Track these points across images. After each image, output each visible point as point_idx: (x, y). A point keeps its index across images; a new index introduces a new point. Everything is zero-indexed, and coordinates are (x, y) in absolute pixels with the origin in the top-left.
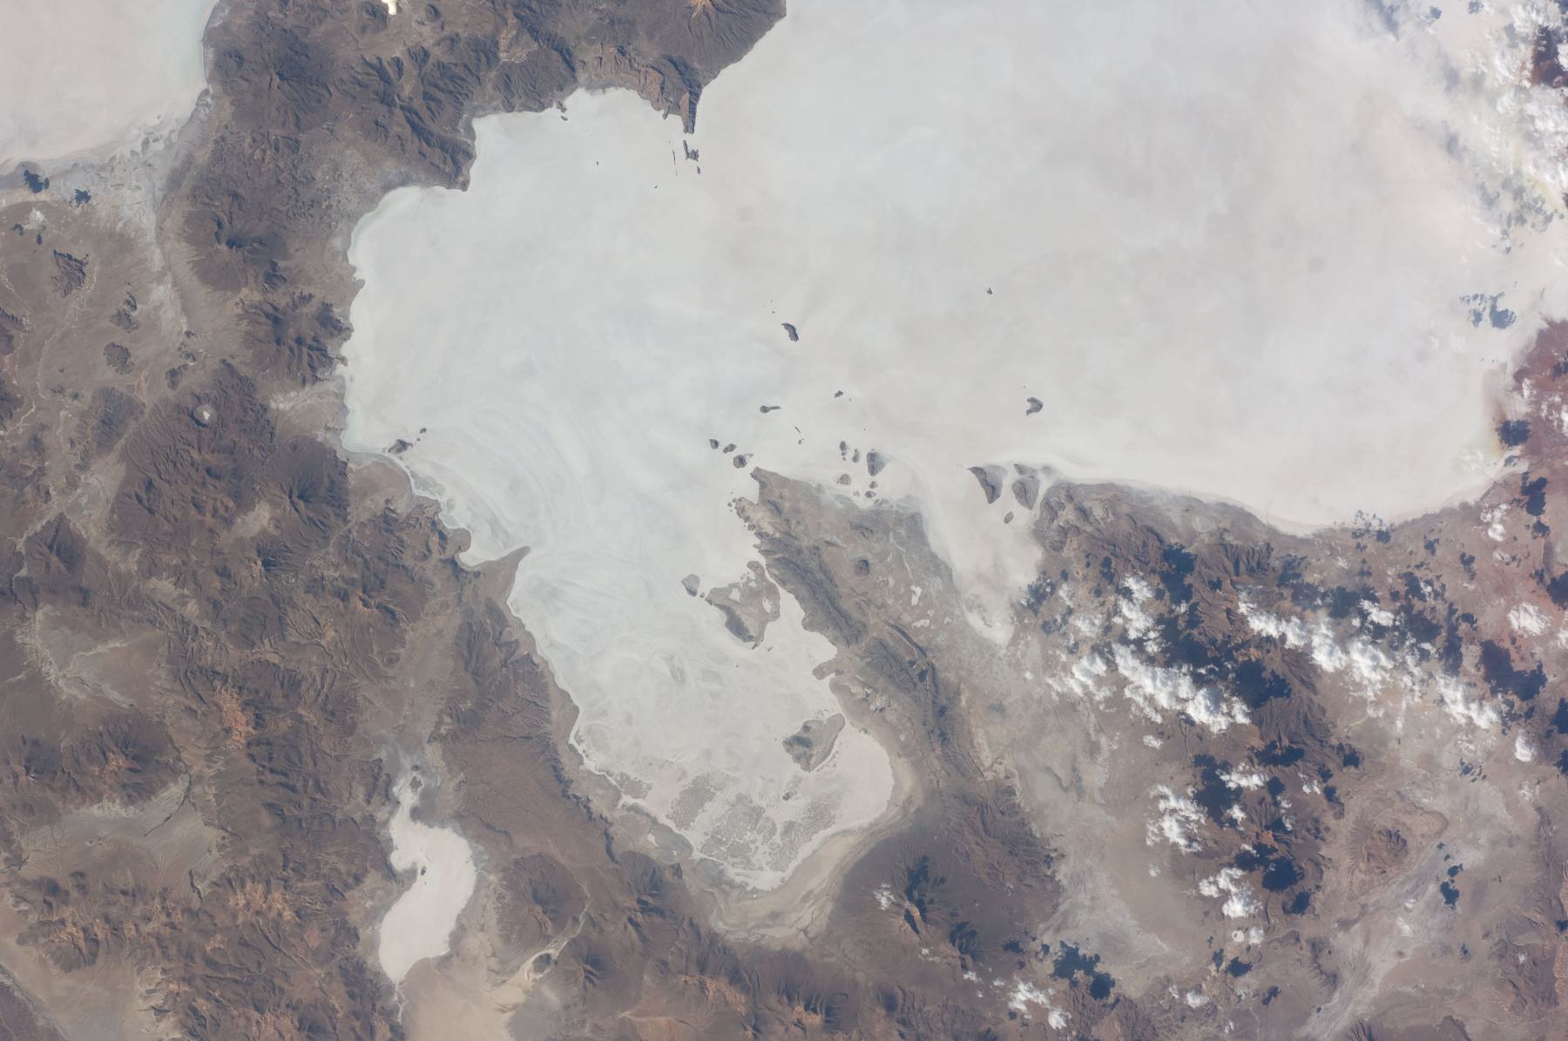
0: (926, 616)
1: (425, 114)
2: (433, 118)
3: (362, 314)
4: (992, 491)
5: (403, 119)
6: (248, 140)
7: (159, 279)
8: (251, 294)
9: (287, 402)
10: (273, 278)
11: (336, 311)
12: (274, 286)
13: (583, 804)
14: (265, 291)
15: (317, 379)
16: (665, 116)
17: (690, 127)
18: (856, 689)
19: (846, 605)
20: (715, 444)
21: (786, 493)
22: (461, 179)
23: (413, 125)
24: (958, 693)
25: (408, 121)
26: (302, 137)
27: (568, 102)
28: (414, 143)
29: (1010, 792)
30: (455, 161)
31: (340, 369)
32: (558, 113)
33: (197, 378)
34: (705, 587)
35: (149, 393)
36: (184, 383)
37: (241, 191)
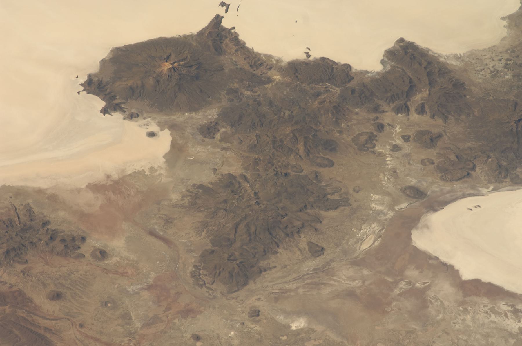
22: (402, 44)
27: (302, 57)
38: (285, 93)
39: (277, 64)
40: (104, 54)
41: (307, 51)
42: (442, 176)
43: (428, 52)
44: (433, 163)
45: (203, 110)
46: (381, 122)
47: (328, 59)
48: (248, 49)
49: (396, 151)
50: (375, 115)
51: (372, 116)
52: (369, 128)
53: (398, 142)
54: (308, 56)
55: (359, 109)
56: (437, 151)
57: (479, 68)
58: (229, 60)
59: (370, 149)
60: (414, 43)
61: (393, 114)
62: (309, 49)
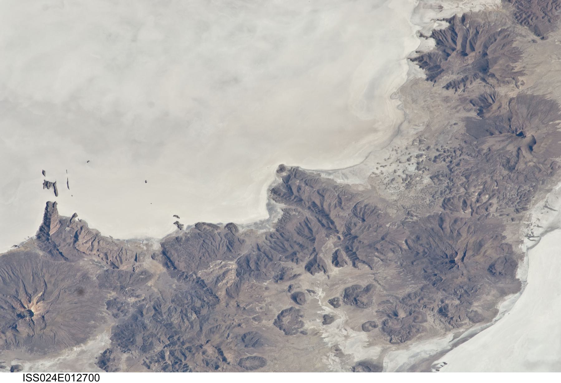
1: (315, 225)
2: (307, 222)
5: (336, 224)
6: (492, 210)
8: (507, 91)
10: (483, 104)
11: (422, 74)
12: (483, 99)
14: (493, 96)
16: (74, 216)
17: (50, 208)
22: (284, 174)
23: (327, 216)
25: (333, 223)
26: (438, 210)
28: (329, 202)
30: (290, 188)
32: (181, 221)
37: (505, 172)
38: (174, 286)
39: (147, 250)
41: (176, 219)
42: (391, 340)
43: (319, 175)
44: (375, 326)
45: (91, 338)
46: (298, 290)
47: (204, 224)
48: (104, 239)
49: (330, 323)
50: (288, 283)
51: (285, 285)
52: (288, 304)
53: (328, 310)
54: (180, 226)
55: (268, 281)
56: (376, 309)
57: (387, 179)
58: (91, 263)
59: (300, 330)
60: (298, 167)
61: (309, 274)
62: (178, 217)
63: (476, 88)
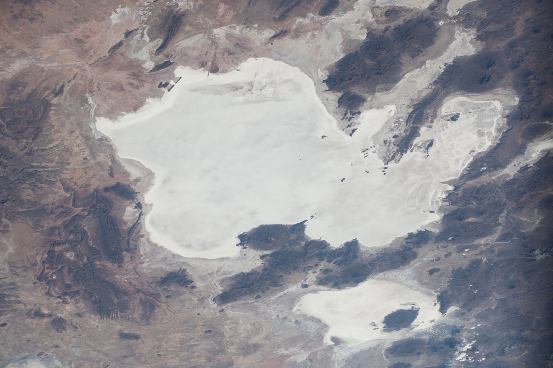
0: (399, 121)
3: (404, 233)
4: (354, 131)
7: (423, 261)
9: (437, 231)
13: (501, 140)
15: (426, 230)
17: (306, 221)
18: (430, 119)
19: (408, 133)
20: (384, 174)
21: (387, 158)
24: (416, 104)
26: (367, 263)
29: (435, 82)
31: (419, 229)
33: (442, 244)
34: (426, 154)
35: (452, 247)
36: (445, 245)
40: (256, 226)
63: (411, 245)
